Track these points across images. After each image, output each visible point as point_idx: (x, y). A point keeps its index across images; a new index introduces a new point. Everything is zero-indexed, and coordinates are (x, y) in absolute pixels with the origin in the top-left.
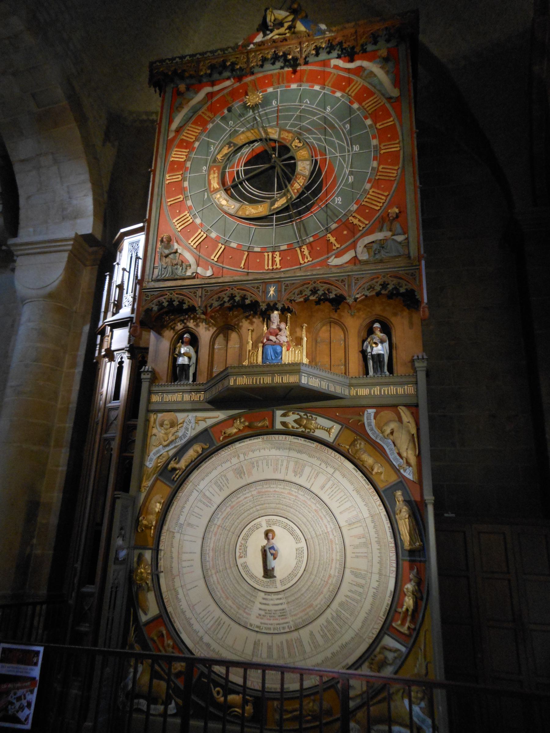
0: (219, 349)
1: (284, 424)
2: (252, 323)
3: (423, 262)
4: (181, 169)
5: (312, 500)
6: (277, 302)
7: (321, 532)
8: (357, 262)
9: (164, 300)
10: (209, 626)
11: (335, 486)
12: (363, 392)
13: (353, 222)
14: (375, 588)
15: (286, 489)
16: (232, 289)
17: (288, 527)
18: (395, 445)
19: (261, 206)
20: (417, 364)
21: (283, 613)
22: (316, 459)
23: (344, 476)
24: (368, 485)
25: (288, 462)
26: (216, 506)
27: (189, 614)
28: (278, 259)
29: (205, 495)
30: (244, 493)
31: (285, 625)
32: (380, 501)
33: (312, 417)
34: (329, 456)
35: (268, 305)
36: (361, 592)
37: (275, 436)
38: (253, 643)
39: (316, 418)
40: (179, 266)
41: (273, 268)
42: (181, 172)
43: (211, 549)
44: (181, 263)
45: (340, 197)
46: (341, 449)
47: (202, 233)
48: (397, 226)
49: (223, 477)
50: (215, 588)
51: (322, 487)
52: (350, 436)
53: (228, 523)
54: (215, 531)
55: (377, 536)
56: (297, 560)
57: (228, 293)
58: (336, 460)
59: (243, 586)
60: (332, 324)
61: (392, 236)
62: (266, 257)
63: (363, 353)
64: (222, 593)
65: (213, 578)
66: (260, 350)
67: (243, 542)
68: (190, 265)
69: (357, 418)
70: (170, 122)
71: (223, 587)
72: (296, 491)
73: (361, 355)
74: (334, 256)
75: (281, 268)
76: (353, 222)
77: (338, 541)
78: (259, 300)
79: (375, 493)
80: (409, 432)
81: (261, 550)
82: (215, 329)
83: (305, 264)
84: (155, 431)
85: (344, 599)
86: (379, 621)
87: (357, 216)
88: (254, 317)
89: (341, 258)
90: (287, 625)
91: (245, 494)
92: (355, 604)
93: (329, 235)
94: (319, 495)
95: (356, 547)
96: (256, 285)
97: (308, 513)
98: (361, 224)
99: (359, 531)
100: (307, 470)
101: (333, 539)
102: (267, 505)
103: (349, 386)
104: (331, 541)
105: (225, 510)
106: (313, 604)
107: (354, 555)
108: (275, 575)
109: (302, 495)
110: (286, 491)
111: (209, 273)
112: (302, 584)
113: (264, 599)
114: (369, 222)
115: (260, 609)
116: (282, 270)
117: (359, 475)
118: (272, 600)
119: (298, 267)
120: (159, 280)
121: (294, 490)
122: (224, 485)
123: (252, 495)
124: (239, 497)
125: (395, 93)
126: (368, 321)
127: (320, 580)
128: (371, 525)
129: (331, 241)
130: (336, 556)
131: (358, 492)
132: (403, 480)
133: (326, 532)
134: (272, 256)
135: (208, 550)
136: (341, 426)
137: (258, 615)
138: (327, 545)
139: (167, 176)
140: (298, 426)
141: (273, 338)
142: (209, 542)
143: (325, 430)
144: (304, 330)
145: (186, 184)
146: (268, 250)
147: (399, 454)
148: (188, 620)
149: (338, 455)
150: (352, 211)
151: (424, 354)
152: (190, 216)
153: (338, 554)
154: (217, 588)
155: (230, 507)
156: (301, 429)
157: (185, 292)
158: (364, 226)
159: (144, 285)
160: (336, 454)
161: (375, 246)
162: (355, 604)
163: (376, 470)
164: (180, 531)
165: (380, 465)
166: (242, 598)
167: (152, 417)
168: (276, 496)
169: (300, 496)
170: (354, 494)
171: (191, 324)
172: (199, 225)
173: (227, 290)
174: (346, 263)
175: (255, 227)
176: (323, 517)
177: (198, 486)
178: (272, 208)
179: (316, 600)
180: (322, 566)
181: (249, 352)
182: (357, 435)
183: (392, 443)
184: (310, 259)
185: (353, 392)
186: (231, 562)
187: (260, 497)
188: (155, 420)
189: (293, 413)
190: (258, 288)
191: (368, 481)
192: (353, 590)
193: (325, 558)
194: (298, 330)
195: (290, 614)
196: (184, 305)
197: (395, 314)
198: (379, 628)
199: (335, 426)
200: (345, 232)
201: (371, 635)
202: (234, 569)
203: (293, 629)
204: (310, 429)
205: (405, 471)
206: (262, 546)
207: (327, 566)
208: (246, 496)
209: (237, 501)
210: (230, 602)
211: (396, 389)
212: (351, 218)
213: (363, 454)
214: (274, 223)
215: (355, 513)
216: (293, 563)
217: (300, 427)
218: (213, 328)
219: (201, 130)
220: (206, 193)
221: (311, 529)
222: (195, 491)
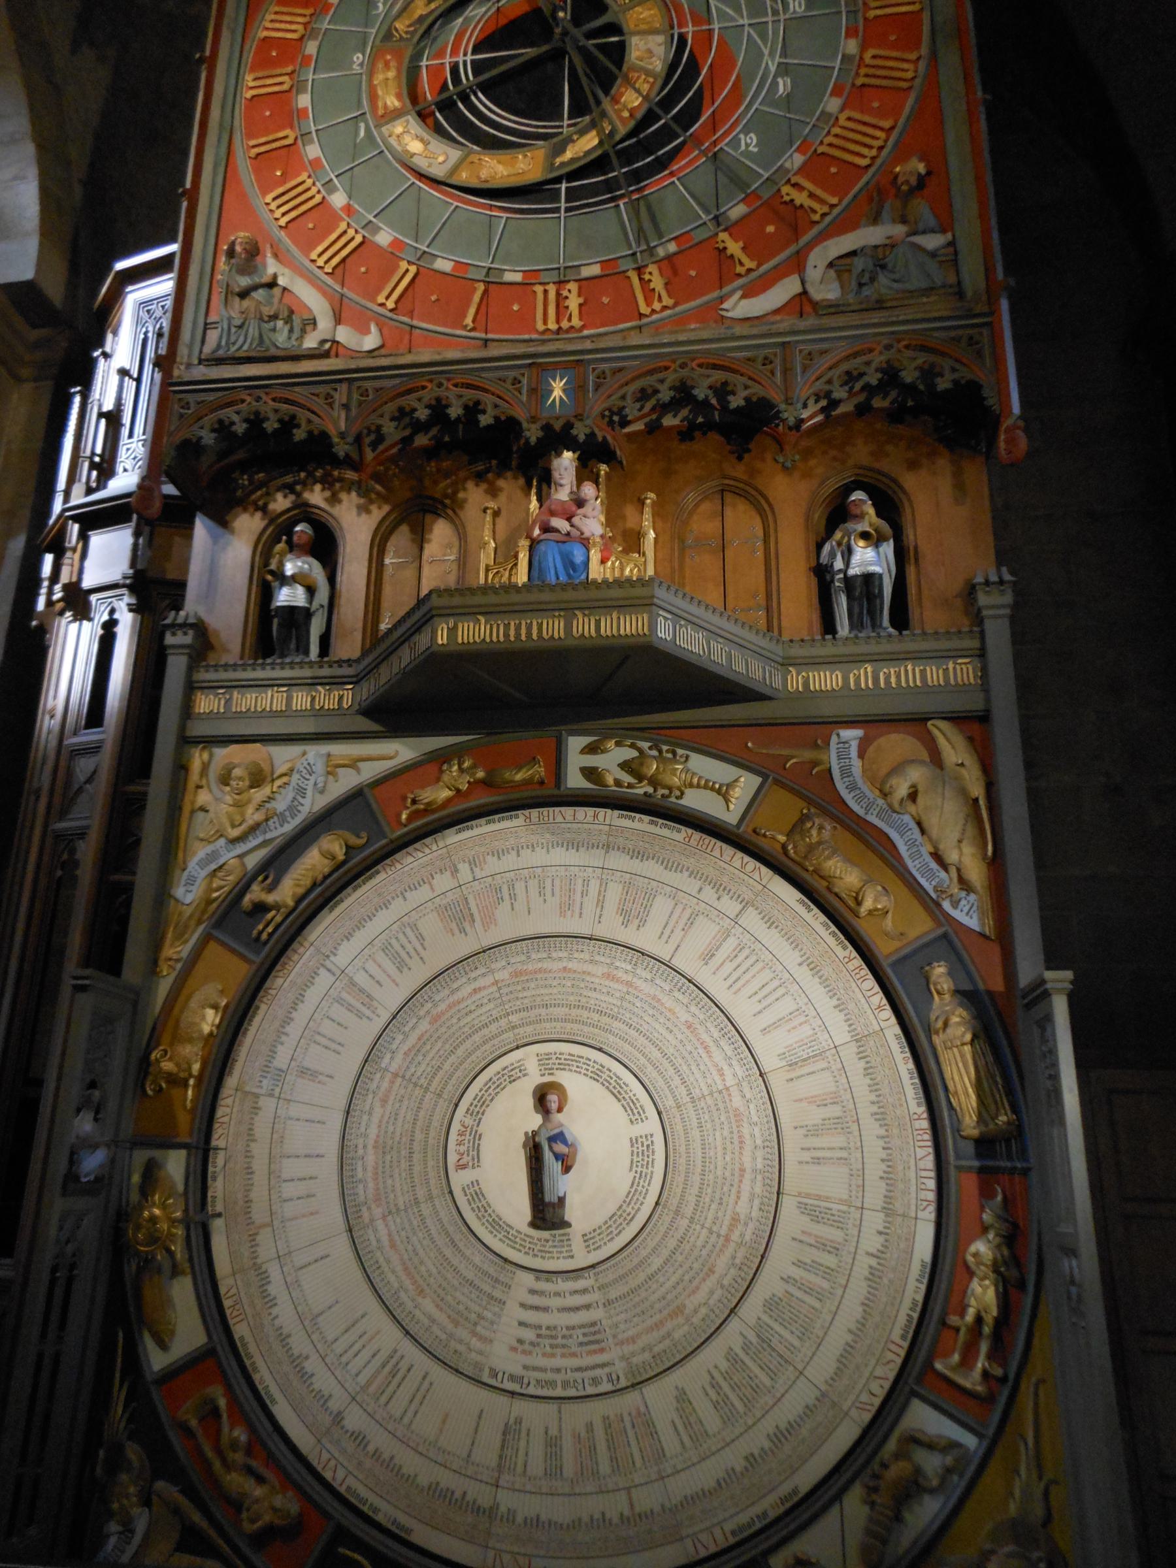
0: (398, 566)
1: (590, 773)
2: (493, 492)
3: (1004, 305)
4: (292, 60)
5: (676, 994)
6: (573, 420)
7: (704, 1088)
8: (808, 308)
9: (236, 418)
10: (362, 1379)
11: (746, 952)
12: (827, 680)
13: (792, 201)
14: (872, 1255)
15: (596, 962)
16: (440, 385)
17: (604, 1076)
18: (923, 831)
19: (525, 156)
20: (983, 599)
21: (595, 1333)
22: (686, 874)
23: (771, 923)
24: (845, 948)
25: (603, 884)
26: (385, 1016)
27: (299, 1343)
28: (573, 303)
29: (353, 984)
30: (473, 975)
31: (598, 1372)
32: (881, 995)
33: (674, 753)
34: (726, 866)
35: (547, 428)
36: (833, 1266)
37: (563, 809)
38: (502, 1427)
39: (687, 757)
40: (280, 323)
41: (560, 328)
42: (289, 69)
43: (371, 1142)
44: (286, 314)
45: (752, 135)
46: (763, 843)
47: (351, 232)
48: (921, 208)
49: (408, 931)
50: (381, 1260)
51: (707, 957)
52: (789, 806)
53: (423, 1066)
54: (383, 1089)
55: (875, 1099)
56: (633, 1174)
57: (428, 395)
58: (746, 877)
59: (468, 1253)
60: (729, 497)
61: (909, 235)
62: (540, 296)
63: (822, 573)
64: (404, 1277)
65: (375, 1231)
66: (523, 557)
67: (469, 1121)
68: (314, 319)
69: (808, 755)
71: (406, 1257)
72: (629, 967)
73: (814, 581)
74: (739, 294)
75: (583, 327)
76: (792, 201)
77: (756, 1112)
78: (520, 414)
79: (865, 971)
80: (963, 792)
81: (525, 1145)
82: (386, 508)
83: (655, 317)
84: (203, 797)
85: (779, 1288)
86: (890, 1356)
88: (499, 475)
89: (762, 297)
90: (607, 1370)
91: (475, 979)
92: (817, 1305)
93: (723, 236)
94: (699, 979)
95: (813, 1131)
96: (512, 374)
97: (664, 1032)
98: (816, 205)
99: (819, 1083)
100: (661, 907)
101: (742, 1109)
102: (543, 1011)
103: (782, 665)
104: (737, 1114)
105: (413, 1028)
106: (684, 1306)
107: (806, 1156)
108: (566, 1218)
109: (646, 980)
110: (599, 970)
111: (371, 341)
112: (651, 1244)
113: (533, 1292)
114: (840, 201)
115: (521, 1324)
116: (586, 332)
117: (815, 919)
118: (557, 1294)
119: (634, 323)
120: (219, 361)
121: (623, 965)
122: (413, 953)
123: (496, 982)
124: (457, 989)
126: (833, 484)
127: (705, 1231)
128: (856, 1068)
129: (729, 252)
130: (754, 1159)
131: (814, 969)
132: (950, 931)
133: (720, 1087)
134: (558, 294)
135: (360, 1146)
136: (758, 780)
137: (515, 1344)
138: (726, 1127)
139: (249, 79)
140: (633, 780)
141: (559, 523)
142: (364, 1124)
143: (712, 789)
144: (647, 510)
145: (304, 101)
146: (544, 277)
147: (937, 857)
148: (297, 1362)
149: (752, 863)
150: (788, 171)
151: (1004, 569)
152: (314, 184)
153: (760, 1154)
154: (388, 1261)
155: (428, 1019)
156: (642, 789)
157: (299, 394)
158: (826, 209)
159: (176, 373)
160: (747, 859)
161: (859, 263)
162: (817, 1305)
163: (868, 904)
164: (278, 1090)
165: (879, 888)
166: (466, 1290)
167: (197, 758)
168: (569, 984)
169: (639, 983)
170: (803, 974)
171: (316, 497)
172: (342, 209)
173: (424, 388)
174: (777, 311)
175: (505, 215)
176: (711, 1044)
177: (332, 958)
178: (558, 161)
179: (694, 1292)
180: (709, 1191)
181: (487, 570)
182: (810, 802)
183: (913, 825)
184: (667, 301)
185: (795, 681)
186: (432, 1182)
187: (519, 988)
188: (205, 767)
189: (618, 744)
190: (516, 381)
191: (842, 937)
192: (808, 1261)
193: (720, 1164)
194: (630, 511)
195: (614, 1336)
196: (295, 431)
197: (913, 465)
198: (892, 1376)
199: (742, 779)
200: (770, 229)
201: (864, 1398)
202: (442, 1205)
203: (623, 1383)
204: (670, 789)
205: (955, 904)
206: (526, 1134)
207: (725, 1189)
208: (476, 985)
209: (451, 999)
210: (428, 1305)
211: (923, 672)
212: (786, 189)
213: (829, 858)
214: (563, 205)
215: (806, 1031)
216: (622, 1181)
217: (640, 781)
218: (380, 508)
220: (362, 125)
221: (677, 1081)
222: (322, 971)
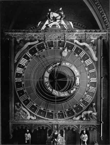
70: (15, 55)
74: (75, 117)
87: (82, 104)
125: (95, 59)
134: (56, 115)
212: (80, 104)
219: (27, 61)
